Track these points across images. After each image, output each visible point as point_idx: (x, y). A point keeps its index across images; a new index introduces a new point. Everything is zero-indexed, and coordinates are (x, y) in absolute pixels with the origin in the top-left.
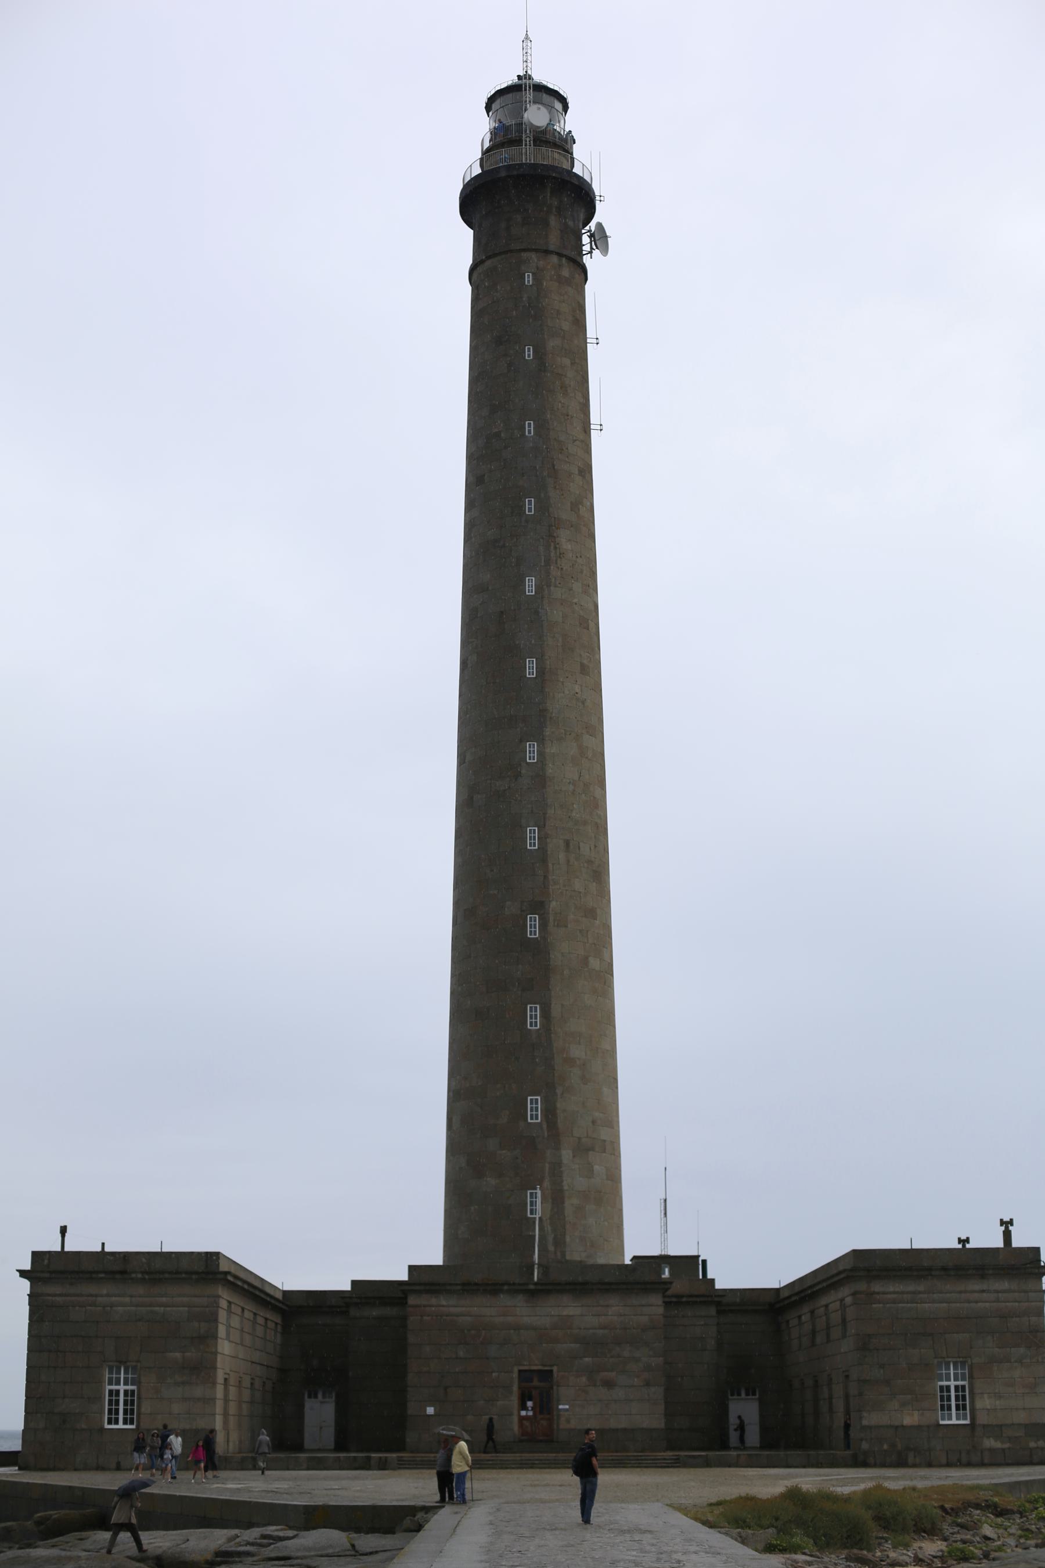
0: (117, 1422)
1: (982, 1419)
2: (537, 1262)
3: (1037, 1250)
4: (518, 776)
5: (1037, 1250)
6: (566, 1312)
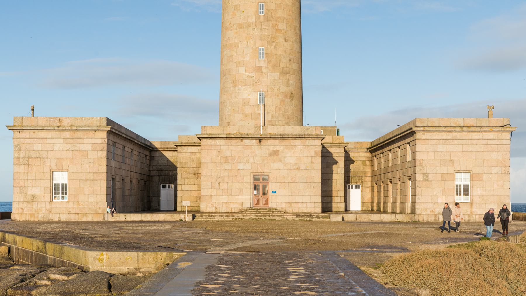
1: (476, 200)
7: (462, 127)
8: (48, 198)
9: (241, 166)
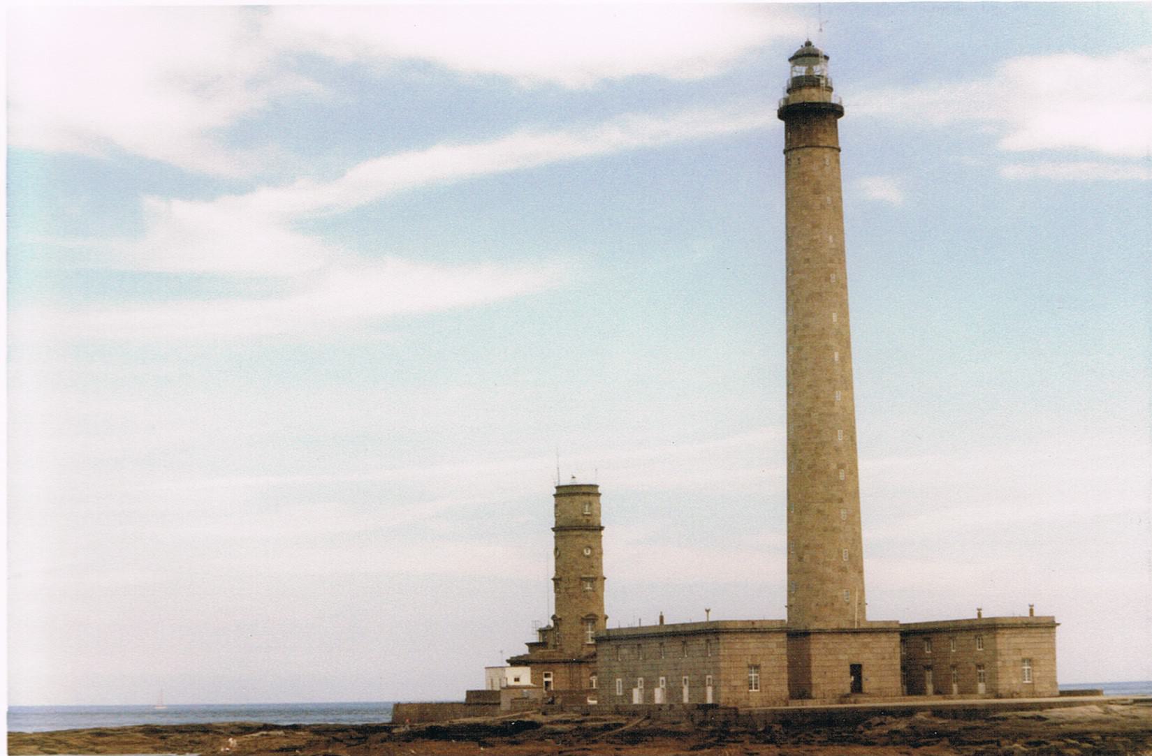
1: (1036, 681)
3: (1053, 617)
7: (1026, 624)
8: (746, 689)
9: (841, 657)
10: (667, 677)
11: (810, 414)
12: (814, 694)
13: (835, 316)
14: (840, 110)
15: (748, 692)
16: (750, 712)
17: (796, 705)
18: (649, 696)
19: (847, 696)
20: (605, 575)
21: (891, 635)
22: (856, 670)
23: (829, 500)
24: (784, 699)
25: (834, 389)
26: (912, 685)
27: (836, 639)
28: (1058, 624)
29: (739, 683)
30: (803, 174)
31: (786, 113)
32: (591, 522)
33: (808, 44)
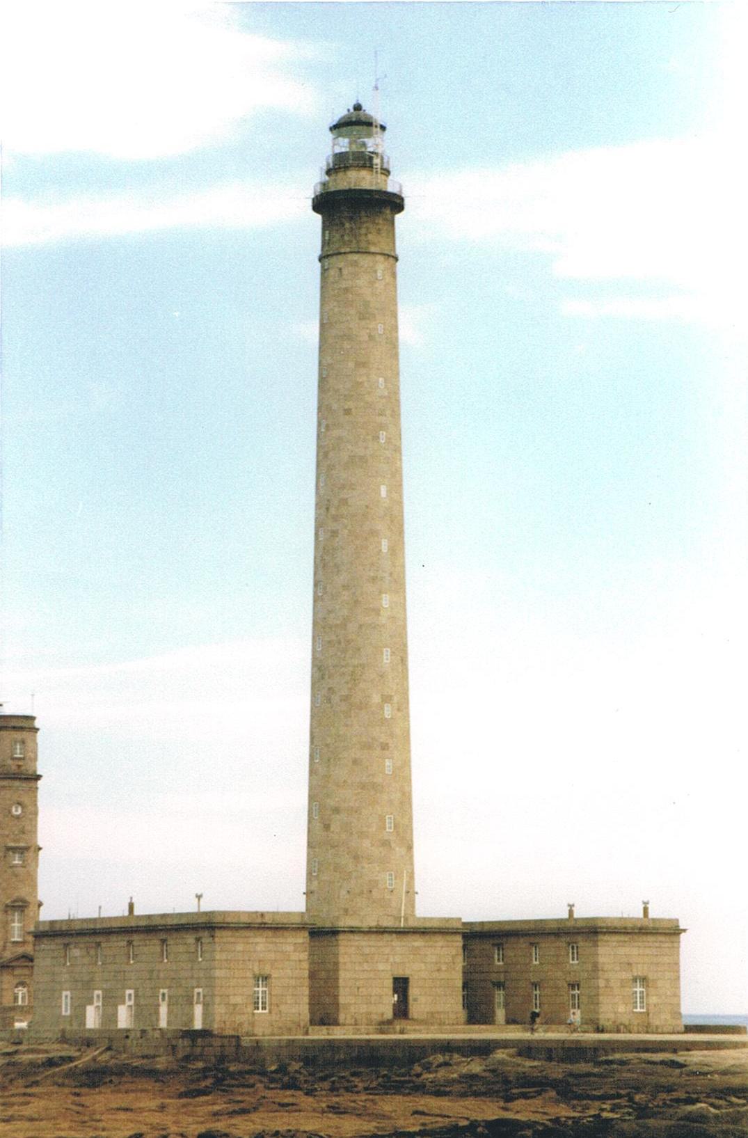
0: (258, 1009)
1: (652, 1011)
2: (403, 915)
3: (677, 920)
4: (378, 614)
5: (677, 920)
6: (416, 944)
7: (640, 929)
8: (250, 1009)
9: (381, 967)
10: (136, 990)
11: (346, 625)
12: (342, 1018)
13: (383, 491)
14: (398, 201)
15: (253, 1014)
16: (257, 1042)
17: (320, 1034)
18: (109, 1017)
19: (389, 1022)
20: (40, 844)
21: (449, 938)
22: (401, 985)
23: (368, 746)
24: (302, 1025)
25: (380, 592)
26: (477, 1011)
27: (373, 941)
28: (684, 930)
29: (238, 1000)
30: (346, 290)
31: (326, 203)
32: (23, 768)
33: (358, 107)
